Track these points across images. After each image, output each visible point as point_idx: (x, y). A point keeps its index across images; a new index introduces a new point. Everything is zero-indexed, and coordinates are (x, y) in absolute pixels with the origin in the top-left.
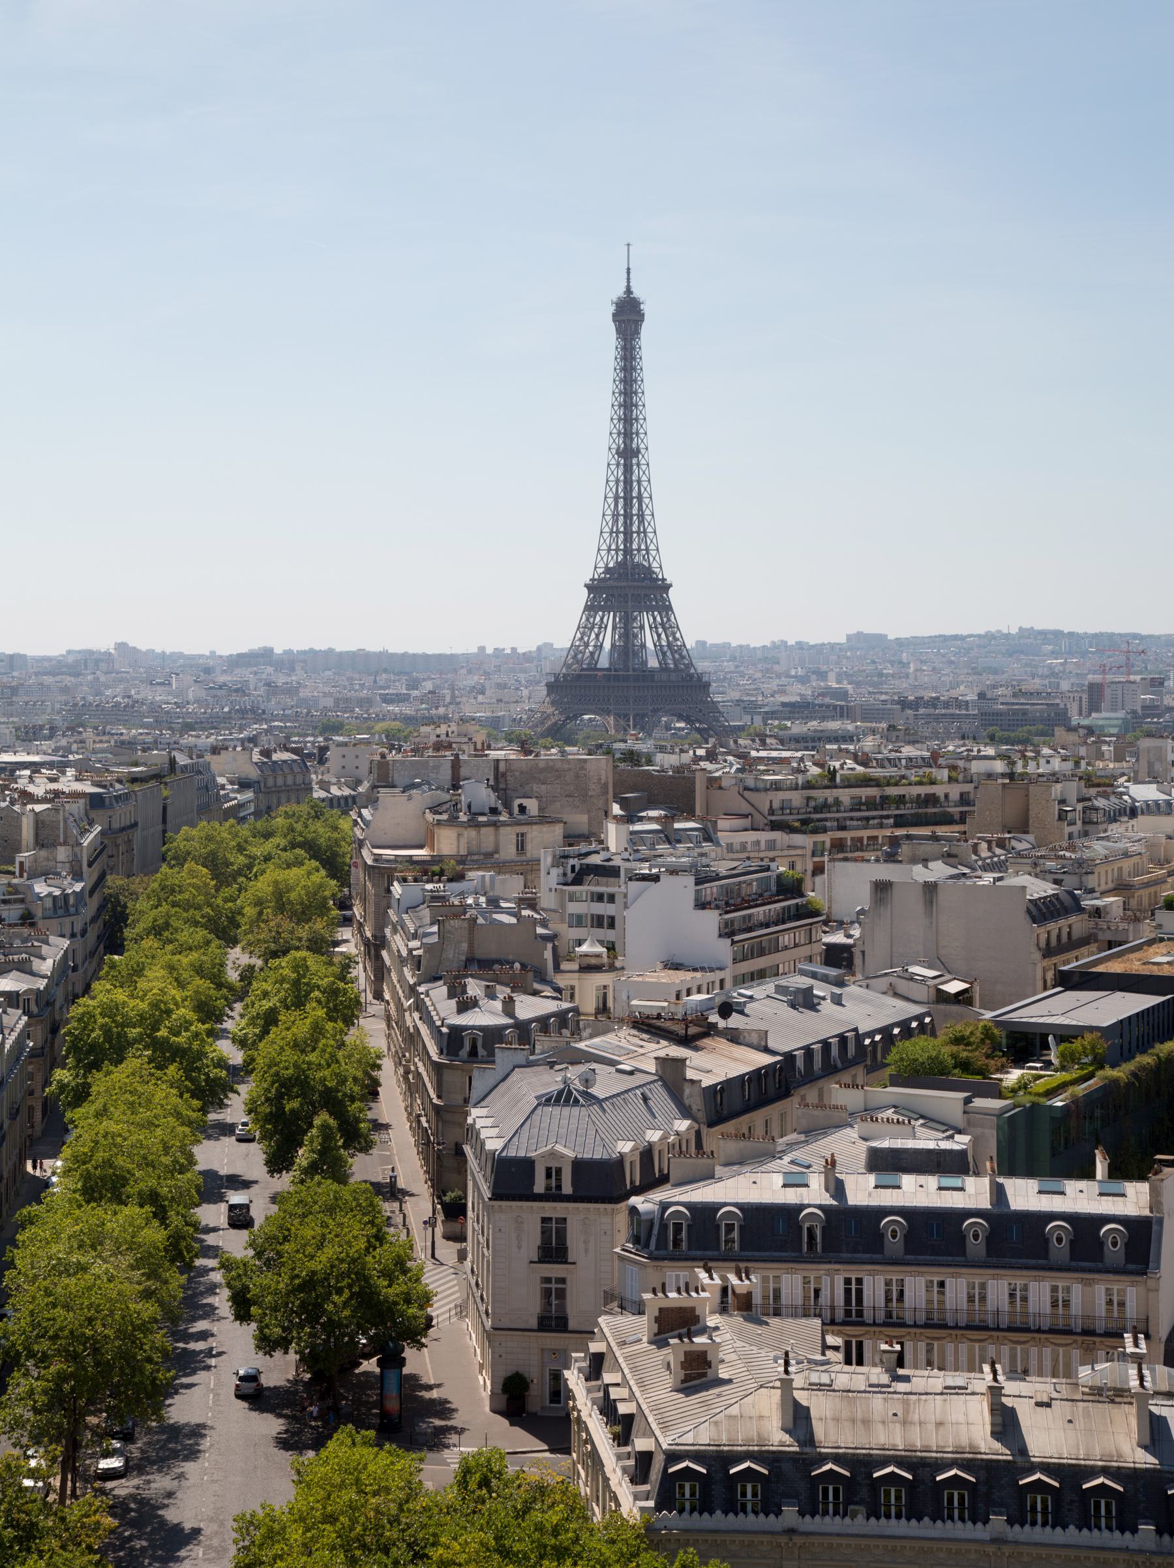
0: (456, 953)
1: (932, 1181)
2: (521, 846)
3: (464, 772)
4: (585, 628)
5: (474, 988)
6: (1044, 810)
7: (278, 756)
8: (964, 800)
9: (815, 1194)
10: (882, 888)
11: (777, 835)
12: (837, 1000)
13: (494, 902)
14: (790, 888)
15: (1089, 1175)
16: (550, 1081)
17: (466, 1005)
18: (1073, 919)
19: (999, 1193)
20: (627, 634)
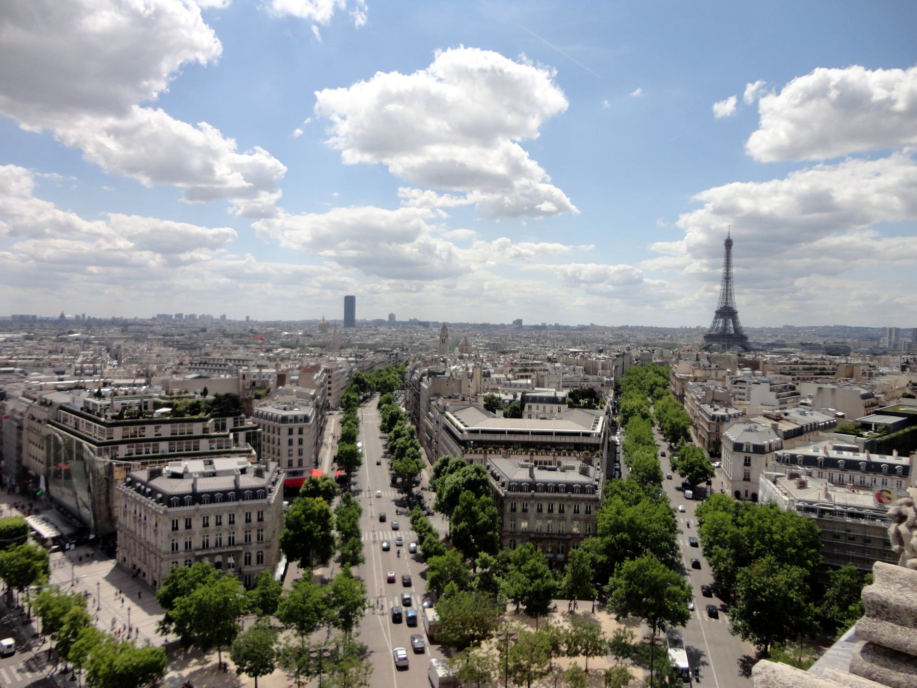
0: (710, 398)
1: (851, 454)
2: (716, 375)
3: (699, 357)
4: (714, 322)
5: (716, 406)
6: (858, 372)
7: (645, 352)
8: (833, 369)
9: (821, 454)
10: (820, 389)
11: (782, 376)
12: (812, 414)
13: (716, 387)
14: (793, 388)
15: (891, 454)
16: (747, 426)
17: (715, 410)
18: (872, 399)
19: (868, 457)
20: (726, 324)
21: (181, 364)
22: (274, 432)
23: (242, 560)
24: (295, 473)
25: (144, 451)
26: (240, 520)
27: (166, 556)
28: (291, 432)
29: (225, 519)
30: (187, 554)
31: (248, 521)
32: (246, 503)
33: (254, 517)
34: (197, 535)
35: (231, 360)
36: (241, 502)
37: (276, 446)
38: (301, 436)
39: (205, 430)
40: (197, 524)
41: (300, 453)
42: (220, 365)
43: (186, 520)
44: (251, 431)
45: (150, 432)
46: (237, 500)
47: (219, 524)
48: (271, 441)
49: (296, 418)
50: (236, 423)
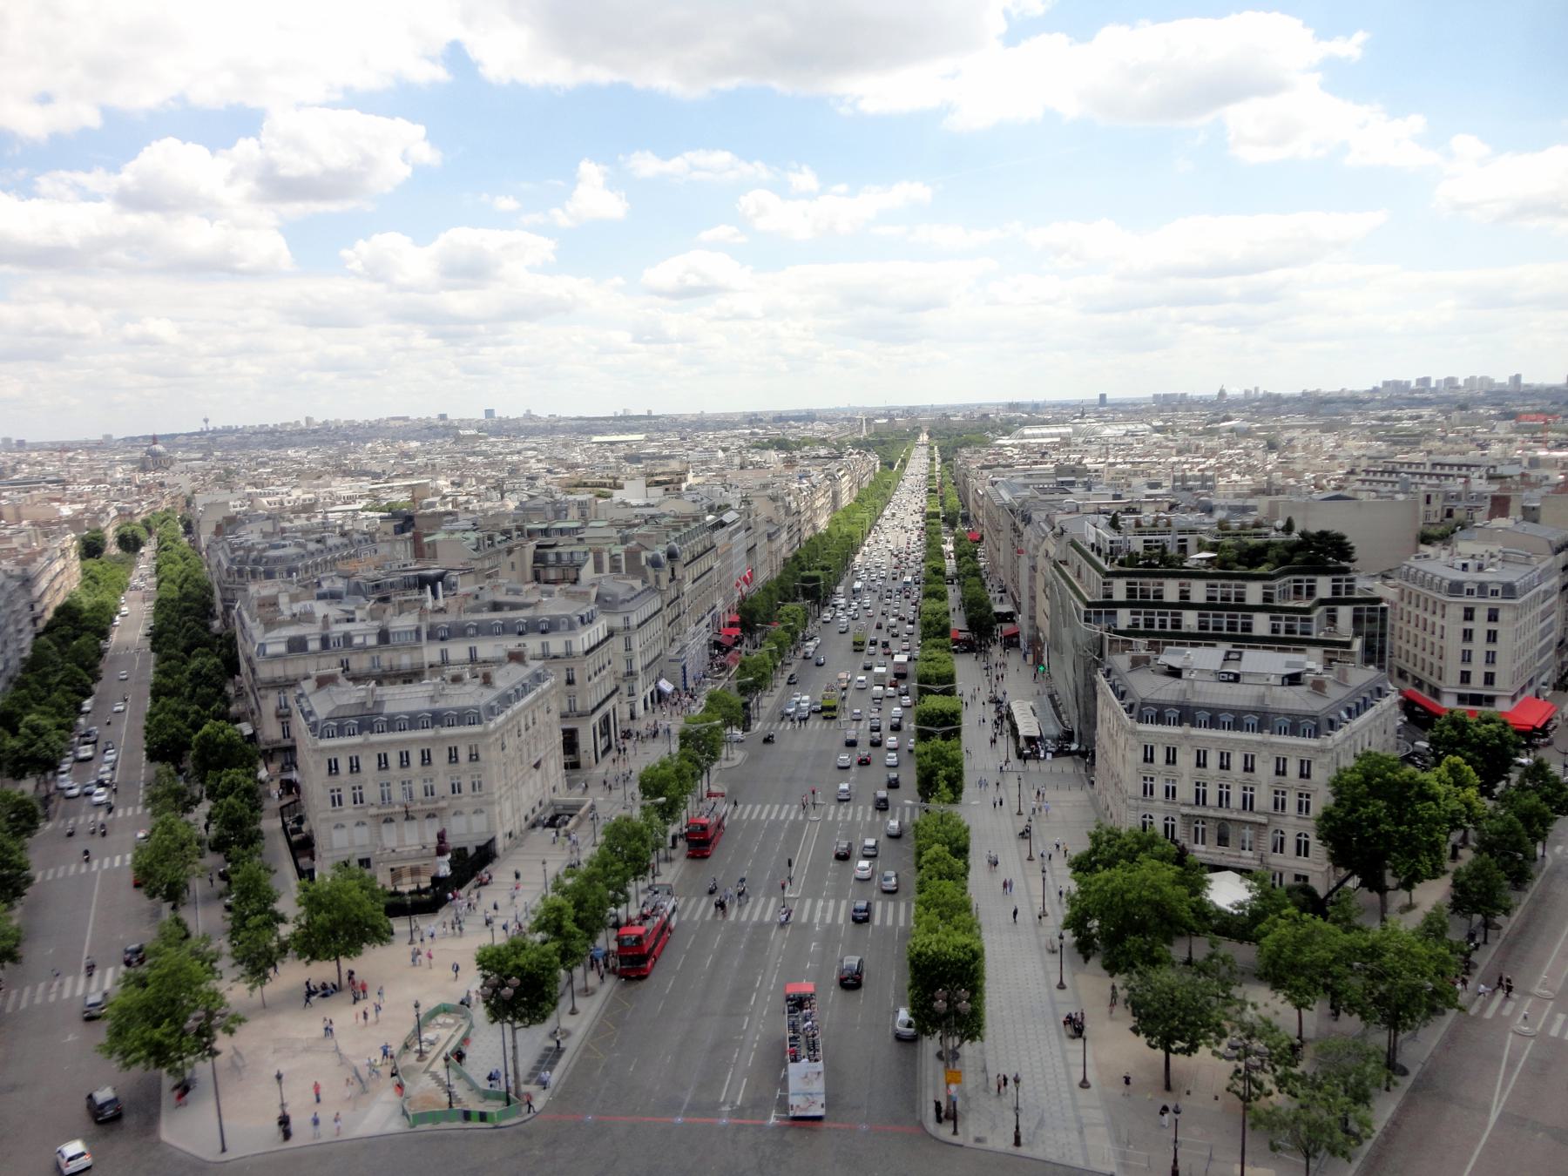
21: (1352, 472)
22: (1434, 613)
23: (1268, 841)
24: (1476, 700)
25: (1157, 623)
26: (1264, 769)
27: (1132, 802)
28: (1469, 614)
29: (1237, 761)
30: (1168, 807)
31: (1280, 772)
32: (1276, 739)
33: (1293, 768)
34: (1186, 778)
35: (1443, 465)
36: (1265, 736)
37: (1436, 638)
38: (1492, 626)
39: (1268, 597)
40: (1186, 760)
41: (1491, 658)
42: (1422, 475)
43: (1168, 749)
44: (1366, 606)
45: (1171, 590)
46: (1260, 731)
47: (1225, 766)
48: (1429, 628)
49: (1482, 587)
50: (1336, 590)
